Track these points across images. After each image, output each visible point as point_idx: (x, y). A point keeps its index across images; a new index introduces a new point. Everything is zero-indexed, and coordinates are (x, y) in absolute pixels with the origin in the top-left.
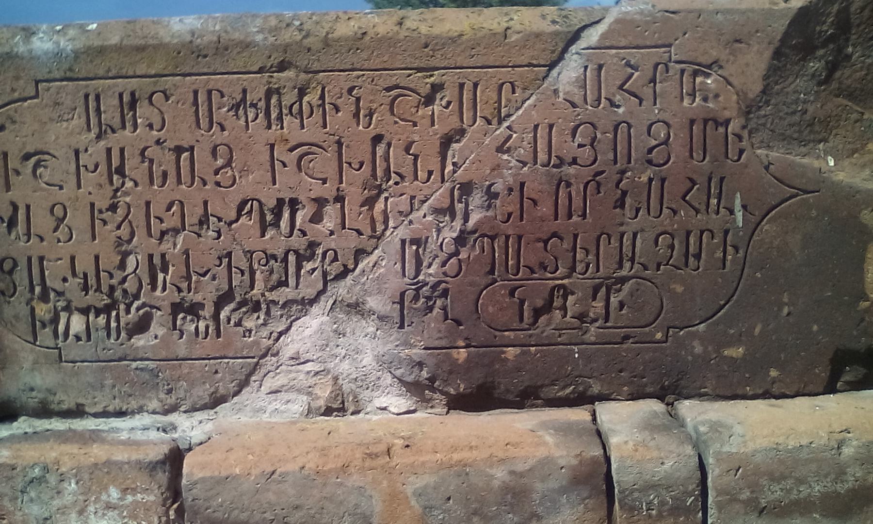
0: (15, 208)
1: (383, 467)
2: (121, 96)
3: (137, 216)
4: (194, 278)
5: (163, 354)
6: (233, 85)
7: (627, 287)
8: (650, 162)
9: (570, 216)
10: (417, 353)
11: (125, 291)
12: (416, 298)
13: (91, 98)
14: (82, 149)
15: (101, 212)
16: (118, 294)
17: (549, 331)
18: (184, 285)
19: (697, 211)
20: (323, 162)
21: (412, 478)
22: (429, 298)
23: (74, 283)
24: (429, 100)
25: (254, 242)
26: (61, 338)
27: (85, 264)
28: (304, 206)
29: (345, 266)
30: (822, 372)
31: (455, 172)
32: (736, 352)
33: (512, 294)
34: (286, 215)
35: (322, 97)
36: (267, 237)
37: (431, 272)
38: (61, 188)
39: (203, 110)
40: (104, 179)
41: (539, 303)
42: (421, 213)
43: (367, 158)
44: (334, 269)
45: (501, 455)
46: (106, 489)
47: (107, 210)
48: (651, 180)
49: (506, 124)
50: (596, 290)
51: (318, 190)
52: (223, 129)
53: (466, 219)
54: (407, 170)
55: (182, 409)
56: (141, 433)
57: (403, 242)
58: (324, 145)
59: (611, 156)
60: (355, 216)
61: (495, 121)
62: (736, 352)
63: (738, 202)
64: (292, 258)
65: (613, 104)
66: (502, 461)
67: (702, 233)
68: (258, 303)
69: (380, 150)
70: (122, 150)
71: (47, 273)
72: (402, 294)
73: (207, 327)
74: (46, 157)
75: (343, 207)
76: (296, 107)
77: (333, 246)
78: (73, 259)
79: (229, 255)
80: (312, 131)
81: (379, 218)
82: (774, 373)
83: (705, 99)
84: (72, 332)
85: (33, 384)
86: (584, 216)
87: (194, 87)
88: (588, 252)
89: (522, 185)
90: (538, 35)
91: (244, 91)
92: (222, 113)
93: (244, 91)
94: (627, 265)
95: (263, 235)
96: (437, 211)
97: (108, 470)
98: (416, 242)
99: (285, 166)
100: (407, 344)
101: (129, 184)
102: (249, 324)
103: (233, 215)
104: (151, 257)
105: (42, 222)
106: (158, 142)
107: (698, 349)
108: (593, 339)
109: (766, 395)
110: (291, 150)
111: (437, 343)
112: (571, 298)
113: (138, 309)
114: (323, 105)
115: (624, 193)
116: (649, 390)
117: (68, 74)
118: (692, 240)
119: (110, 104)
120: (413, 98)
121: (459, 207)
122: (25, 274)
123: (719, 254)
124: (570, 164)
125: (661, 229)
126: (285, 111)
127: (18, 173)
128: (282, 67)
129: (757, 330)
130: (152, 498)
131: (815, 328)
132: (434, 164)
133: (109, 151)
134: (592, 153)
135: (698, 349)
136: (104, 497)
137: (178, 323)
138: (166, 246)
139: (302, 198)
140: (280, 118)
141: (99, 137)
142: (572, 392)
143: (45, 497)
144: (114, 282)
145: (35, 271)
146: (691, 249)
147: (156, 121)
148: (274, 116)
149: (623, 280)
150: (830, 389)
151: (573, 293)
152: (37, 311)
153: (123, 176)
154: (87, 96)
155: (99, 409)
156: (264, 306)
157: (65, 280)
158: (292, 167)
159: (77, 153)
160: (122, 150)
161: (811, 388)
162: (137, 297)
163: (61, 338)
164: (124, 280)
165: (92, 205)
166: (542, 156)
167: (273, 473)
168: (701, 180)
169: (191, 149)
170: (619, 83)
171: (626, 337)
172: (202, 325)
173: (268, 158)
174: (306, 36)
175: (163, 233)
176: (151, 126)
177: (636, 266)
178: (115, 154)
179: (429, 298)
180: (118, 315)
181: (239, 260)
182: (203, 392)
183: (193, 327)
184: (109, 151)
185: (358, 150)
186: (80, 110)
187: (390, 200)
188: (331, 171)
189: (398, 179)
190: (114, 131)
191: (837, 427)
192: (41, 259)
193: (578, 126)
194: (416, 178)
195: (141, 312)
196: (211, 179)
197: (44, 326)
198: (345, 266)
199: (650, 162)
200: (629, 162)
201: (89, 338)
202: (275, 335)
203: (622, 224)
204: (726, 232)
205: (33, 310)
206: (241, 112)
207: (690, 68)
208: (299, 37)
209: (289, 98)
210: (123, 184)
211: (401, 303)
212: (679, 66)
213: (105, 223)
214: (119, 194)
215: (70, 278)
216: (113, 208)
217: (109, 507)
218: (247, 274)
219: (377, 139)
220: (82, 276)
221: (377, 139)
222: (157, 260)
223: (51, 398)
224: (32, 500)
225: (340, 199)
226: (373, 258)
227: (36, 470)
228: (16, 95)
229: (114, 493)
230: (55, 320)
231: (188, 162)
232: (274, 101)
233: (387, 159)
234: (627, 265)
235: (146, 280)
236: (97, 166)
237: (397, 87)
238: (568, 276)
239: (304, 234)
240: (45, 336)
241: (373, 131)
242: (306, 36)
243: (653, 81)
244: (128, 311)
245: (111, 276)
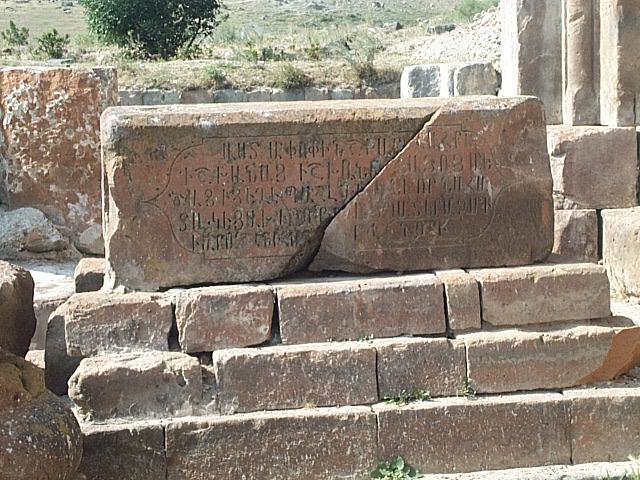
20: (321, 171)
25: (293, 205)
40: (230, 180)
64: (307, 212)
80: (318, 158)
84: (210, 246)
119: (234, 149)
123: (483, 207)
140: (305, 153)
147: (253, 155)
158: (309, 172)
161: (522, 263)
178: (235, 169)
217: (249, 312)
229: (251, 305)
241: (343, 158)
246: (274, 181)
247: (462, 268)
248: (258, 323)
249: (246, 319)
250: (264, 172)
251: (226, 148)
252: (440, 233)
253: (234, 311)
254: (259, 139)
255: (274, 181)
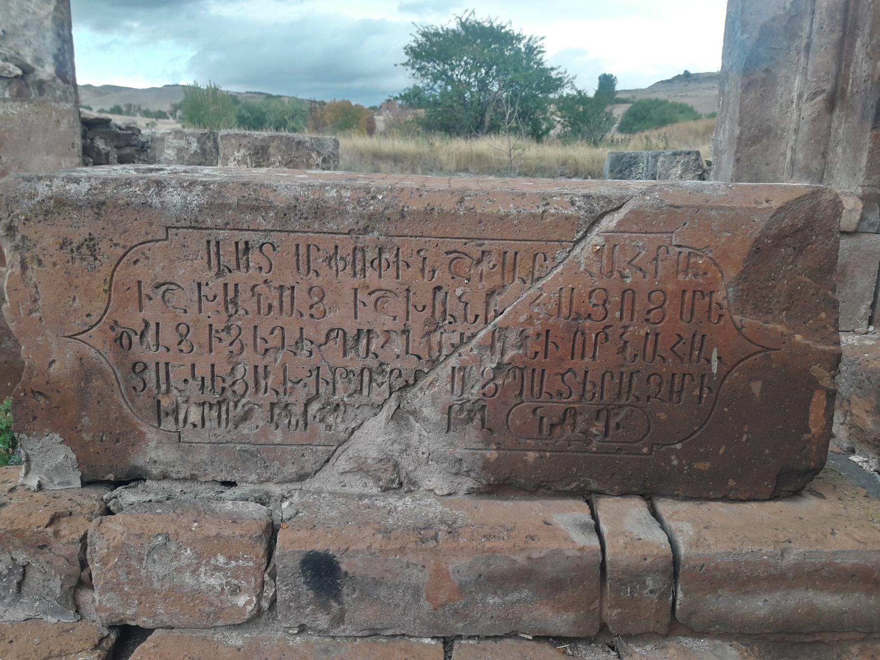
0: (147, 324)
1: (431, 549)
2: (237, 243)
3: (247, 336)
4: (289, 384)
5: (263, 441)
6: (326, 243)
7: (624, 412)
8: (647, 320)
9: (583, 357)
10: (459, 452)
11: (234, 392)
12: (461, 410)
13: (213, 243)
14: (204, 283)
15: (217, 331)
16: (229, 394)
17: (561, 442)
18: (281, 390)
19: (682, 359)
20: (396, 305)
21: (454, 559)
22: (470, 411)
23: (194, 385)
24: (479, 261)
26: (181, 424)
27: (203, 370)
28: (378, 336)
29: (407, 381)
30: (769, 486)
31: (496, 317)
32: (705, 466)
33: (535, 411)
34: (364, 342)
35: (397, 255)
36: (349, 357)
37: (475, 392)
38: (185, 312)
39: (303, 258)
40: (221, 308)
41: (555, 420)
42: (468, 347)
43: (429, 302)
44: (398, 383)
45: (521, 545)
46: (215, 556)
47: (223, 330)
48: (647, 334)
49: (540, 284)
50: (599, 412)
51: (390, 324)
52: (318, 275)
53: (502, 354)
54: (458, 313)
55: (275, 480)
56: (241, 508)
57: (454, 368)
58: (397, 292)
59: (618, 314)
60: (417, 344)
61: (529, 282)
62: (705, 466)
63: (715, 355)
64: (366, 374)
65: (623, 276)
66: (522, 550)
67: (684, 375)
68: (338, 405)
69: (440, 296)
70: (236, 285)
71: (171, 375)
72: (450, 407)
73: (297, 422)
74: (173, 287)
75: (408, 337)
76: (376, 262)
77: (399, 366)
78: (193, 366)
79: (318, 368)
80: (388, 281)
81: (435, 347)
82: (731, 483)
83: (695, 275)
85: (156, 458)
86: (594, 357)
87: (297, 242)
88: (594, 386)
89: (548, 331)
90: (567, 218)
91: (336, 247)
92: (318, 262)
93: (336, 247)
94: (624, 397)
95: (345, 355)
96: (480, 346)
97: (219, 543)
98: (463, 368)
99: (365, 305)
100: (451, 444)
101: (241, 312)
102: (330, 419)
103: (323, 339)
104: (256, 367)
105: (169, 336)
106: (266, 282)
107: (675, 462)
108: (594, 449)
109: (725, 499)
110: (370, 294)
111: (474, 446)
112: (579, 418)
113: (243, 406)
114: (398, 261)
115: (626, 342)
116: (634, 489)
117: (193, 224)
118: (676, 381)
119: (228, 250)
120: (468, 260)
121: (498, 345)
122: (153, 374)
124: (586, 319)
125: (653, 372)
126: (368, 265)
127: (150, 299)
128: (366, 230)
129: (721, 452)
130: (251, 564)
131: (767, 451)
132: (480, 310)
133: (226, 285)
134: (603, 311)
135: (675, 462)
136: (213, 562)
137: (275, 418)
138: (268, 359)
139: (377, 330)
140: (364, 270)
141: (219, 274)
142: (576, 486)
143: (166, 559)
144: (226, 385)
145: (162, 374)
146: (676, 388)
147: (265, 265)
148: (359, 267)
149: (620, 407)
150: (774, 497)
151: (581, 414)
152: (163, 403)
153: (236, 304)
154: (208, 242)
155: (209, 478)
156: (342, 408)
157: (186, 381)
158: (371, 306)
159: (199, 285)
160: (236, 285)
162: (243, 396)
163: (181, 424)
164: (234, 383)
165: (211, 326)
166: (565, 311)
167: (347, 549)
168: (687, 336)
169: (293, 288)
170: (628, 259)
171: (619, 450)
172: (293, 422)
173: (352, 299)
174: (386, 208)
175: (267, 350)
176: (260, 268)
177: (632, 397)
178: (231, 288)
179: (470, 411)
180: (227, 410)
181: (325, 373)
182: (291, 470)
183: (287, 421)
184: (226, 285)
185: (424, 297)
186: (203, 253)
187: (444, 335)
188: (401, 313)
189: (452, 320)
190: (230, 271)
191: (781, 536)
192: (167, 364)
193: (594, 290)
194: (466, 319)
195: (246, 408)
196: (307, 313)
197: (167, 414)
198: (407, 381)
199: (647, 320)
200: (632, 320)
201: (203, 425)
202: (350, 430)
203: (622, 366)
204: (703, 376)
205: (159, 402)
206: (333, 263)
207: (686, 251)
208: (381, 209)
209: (370, 255)
210: (237, 311)
211: (449, 413)
212: (678, 249)
213: (220, 340)
214: (232, 319)
215: (190, 380)
216: (228, 328)
217: (216, 568)
218: (331, 384)
219: (438, 288)
220: (200, 379)
221: (438, 288)
222: (261, 370)
223: (170, 469)
224: (154, 561)
225: (406, 331)
226: (429, 379)
227: (160, 539)
228: (150, 237)
229: (221, 559)
230: (176, 411)
231: (289, 299)
232: (359, 256)
233: (444, 303)
234: (624, 397)
235: (251, 384)
236: (215, 297)
237: (455, 252)
238: (579, 401)
239: (377, 356)
240: (168, 424)
241: (435, 282)
242: (386, 208)
243: (656, 259)
244: (236, 406)
245: (224, 380)
246: (306, 317)
247: (643, 496)
248: (236, 591)
249: (212, 581)
250: (286, 299)
251: (213, 249)
252: (606, 434)
253: (189, 566)
254: (274, 237)
255: (306, 317)
